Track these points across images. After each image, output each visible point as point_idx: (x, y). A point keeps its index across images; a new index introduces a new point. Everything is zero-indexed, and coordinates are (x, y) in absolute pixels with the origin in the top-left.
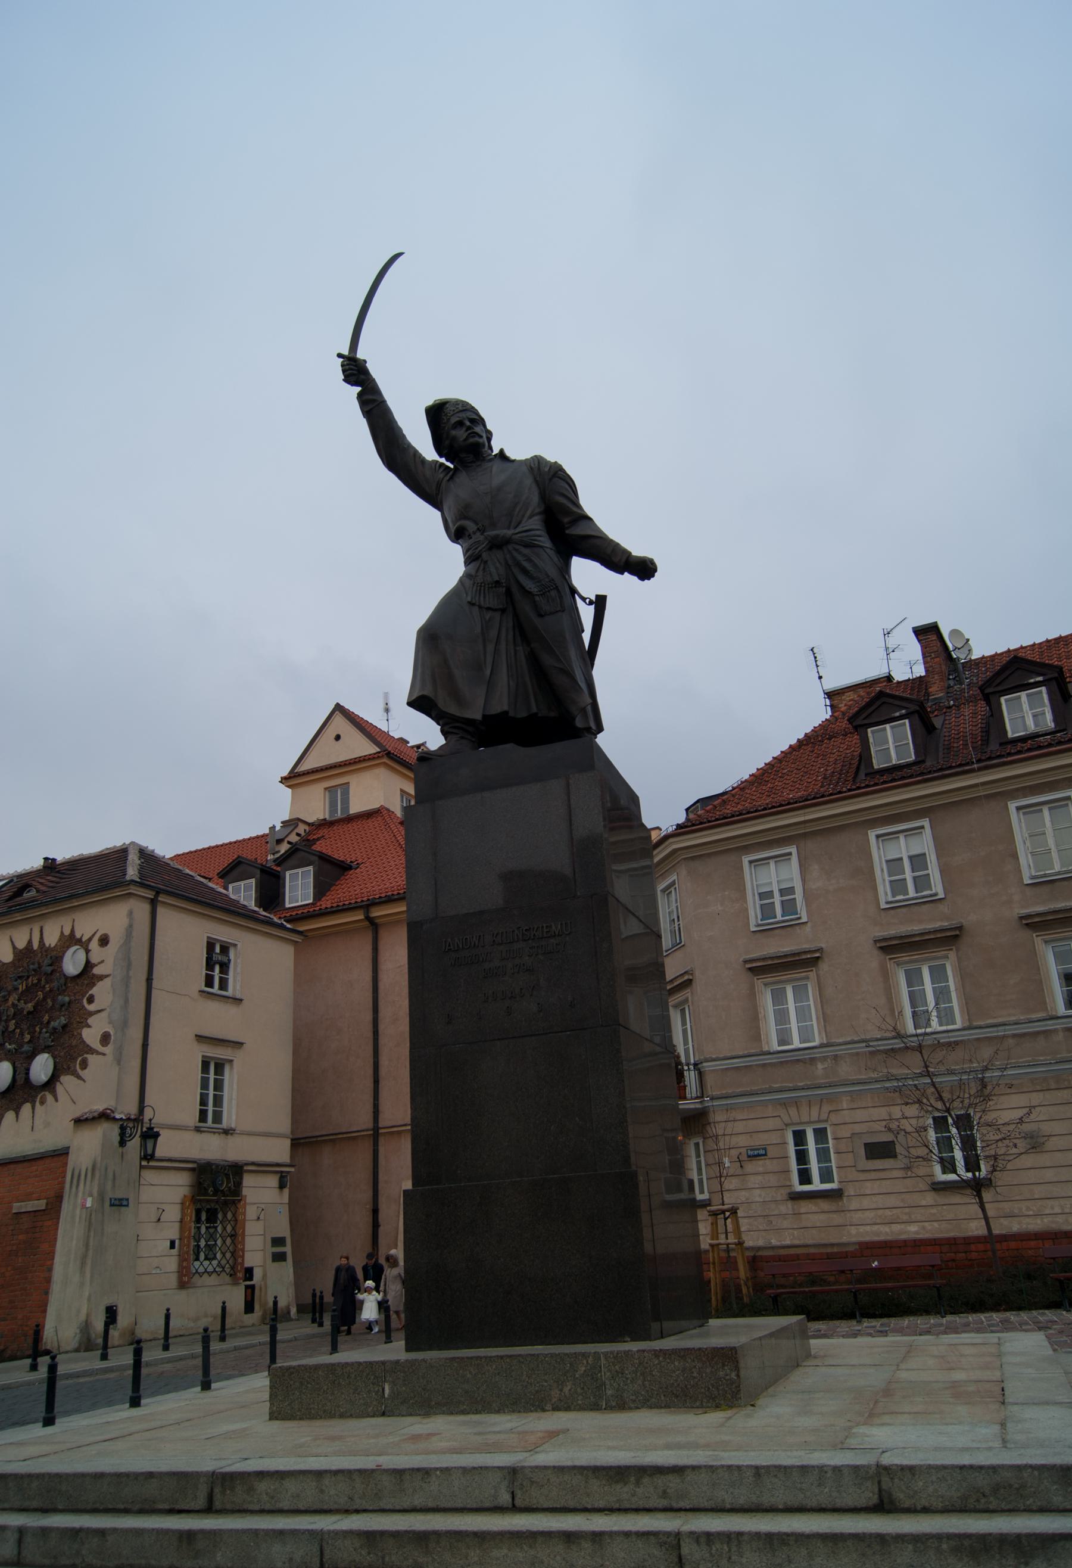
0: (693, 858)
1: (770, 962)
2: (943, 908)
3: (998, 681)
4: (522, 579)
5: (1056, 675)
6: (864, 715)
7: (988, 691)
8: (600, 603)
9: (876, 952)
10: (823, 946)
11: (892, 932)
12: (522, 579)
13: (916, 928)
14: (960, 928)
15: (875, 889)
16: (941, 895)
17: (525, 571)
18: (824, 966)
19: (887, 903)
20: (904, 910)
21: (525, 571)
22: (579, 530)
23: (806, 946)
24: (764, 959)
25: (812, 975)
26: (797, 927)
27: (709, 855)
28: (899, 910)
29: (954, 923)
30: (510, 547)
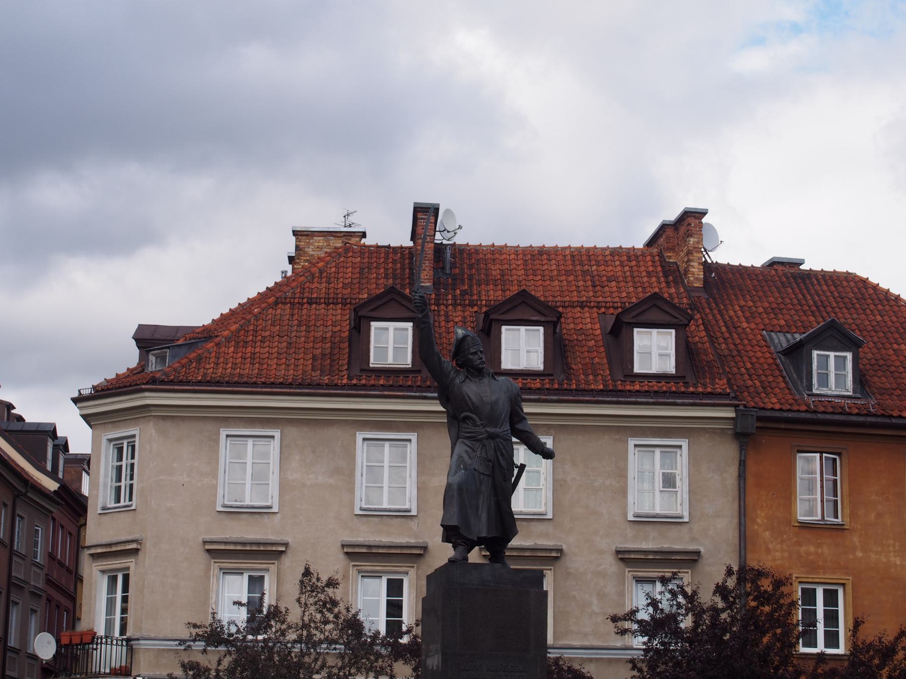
0: (164, 418)
1: (232, 547)
2: (413, 524)
3: (504, 309)
4: (500, 458)
5: (555, 319)
6: (373, 306)
7: (493, 316)
8: (522, 467)
9: (342, 556)
10: (289, 539)
11: (360, 539)
12: (500, 458)
13: (385, 539)
14: (425, 548)
15: (352, 491)
16: (414, 513)
17: (502, 455)
18: (286, 561)
19: (361, 509)
20: (376, 519)
21: (502, 455)
22: (519, 426)
23: (272, 537)
24: (226, 543)
25: (273, 568)
26: (266, 516)
27: (183, 418)
28: (372, 519)
29: (420, 541)
30: (498, 440)
